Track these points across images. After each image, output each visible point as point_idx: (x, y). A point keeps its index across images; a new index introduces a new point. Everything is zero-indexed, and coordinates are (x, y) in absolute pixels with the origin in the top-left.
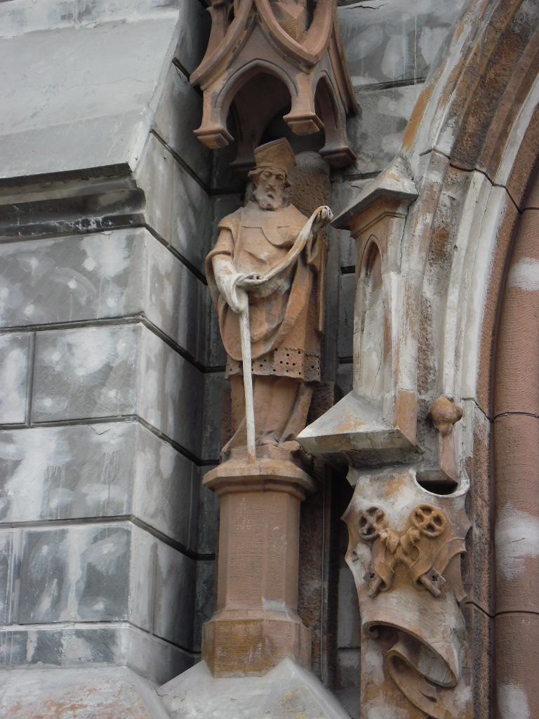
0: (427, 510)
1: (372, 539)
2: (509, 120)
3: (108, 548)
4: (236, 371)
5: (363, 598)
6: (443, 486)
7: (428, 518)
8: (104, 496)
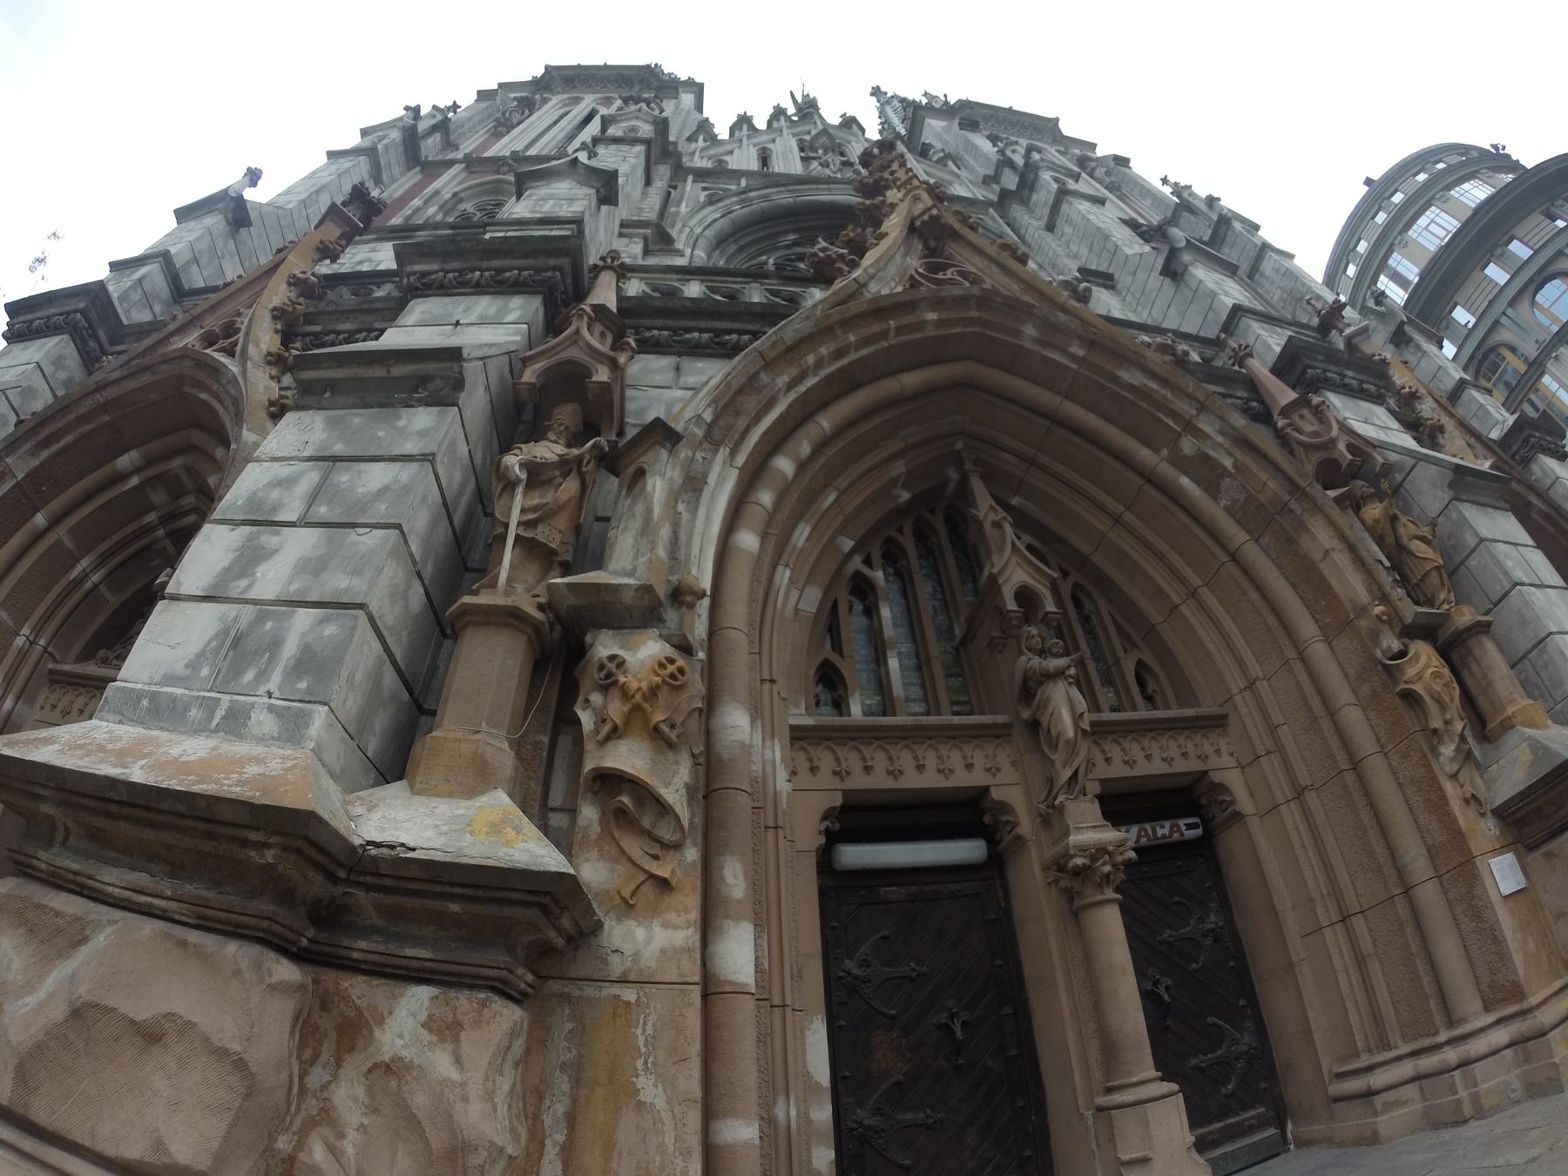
0: (671, 661)
1: (608, 684)
2: (747, 431)
3: (330, 630)
4: (499, 530)
5: (589, 746)
6: (686, 649)
7: (671, 668)
8: (344, 584)
